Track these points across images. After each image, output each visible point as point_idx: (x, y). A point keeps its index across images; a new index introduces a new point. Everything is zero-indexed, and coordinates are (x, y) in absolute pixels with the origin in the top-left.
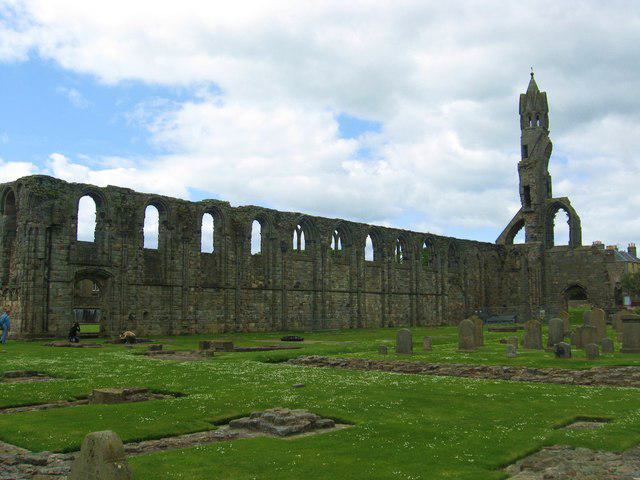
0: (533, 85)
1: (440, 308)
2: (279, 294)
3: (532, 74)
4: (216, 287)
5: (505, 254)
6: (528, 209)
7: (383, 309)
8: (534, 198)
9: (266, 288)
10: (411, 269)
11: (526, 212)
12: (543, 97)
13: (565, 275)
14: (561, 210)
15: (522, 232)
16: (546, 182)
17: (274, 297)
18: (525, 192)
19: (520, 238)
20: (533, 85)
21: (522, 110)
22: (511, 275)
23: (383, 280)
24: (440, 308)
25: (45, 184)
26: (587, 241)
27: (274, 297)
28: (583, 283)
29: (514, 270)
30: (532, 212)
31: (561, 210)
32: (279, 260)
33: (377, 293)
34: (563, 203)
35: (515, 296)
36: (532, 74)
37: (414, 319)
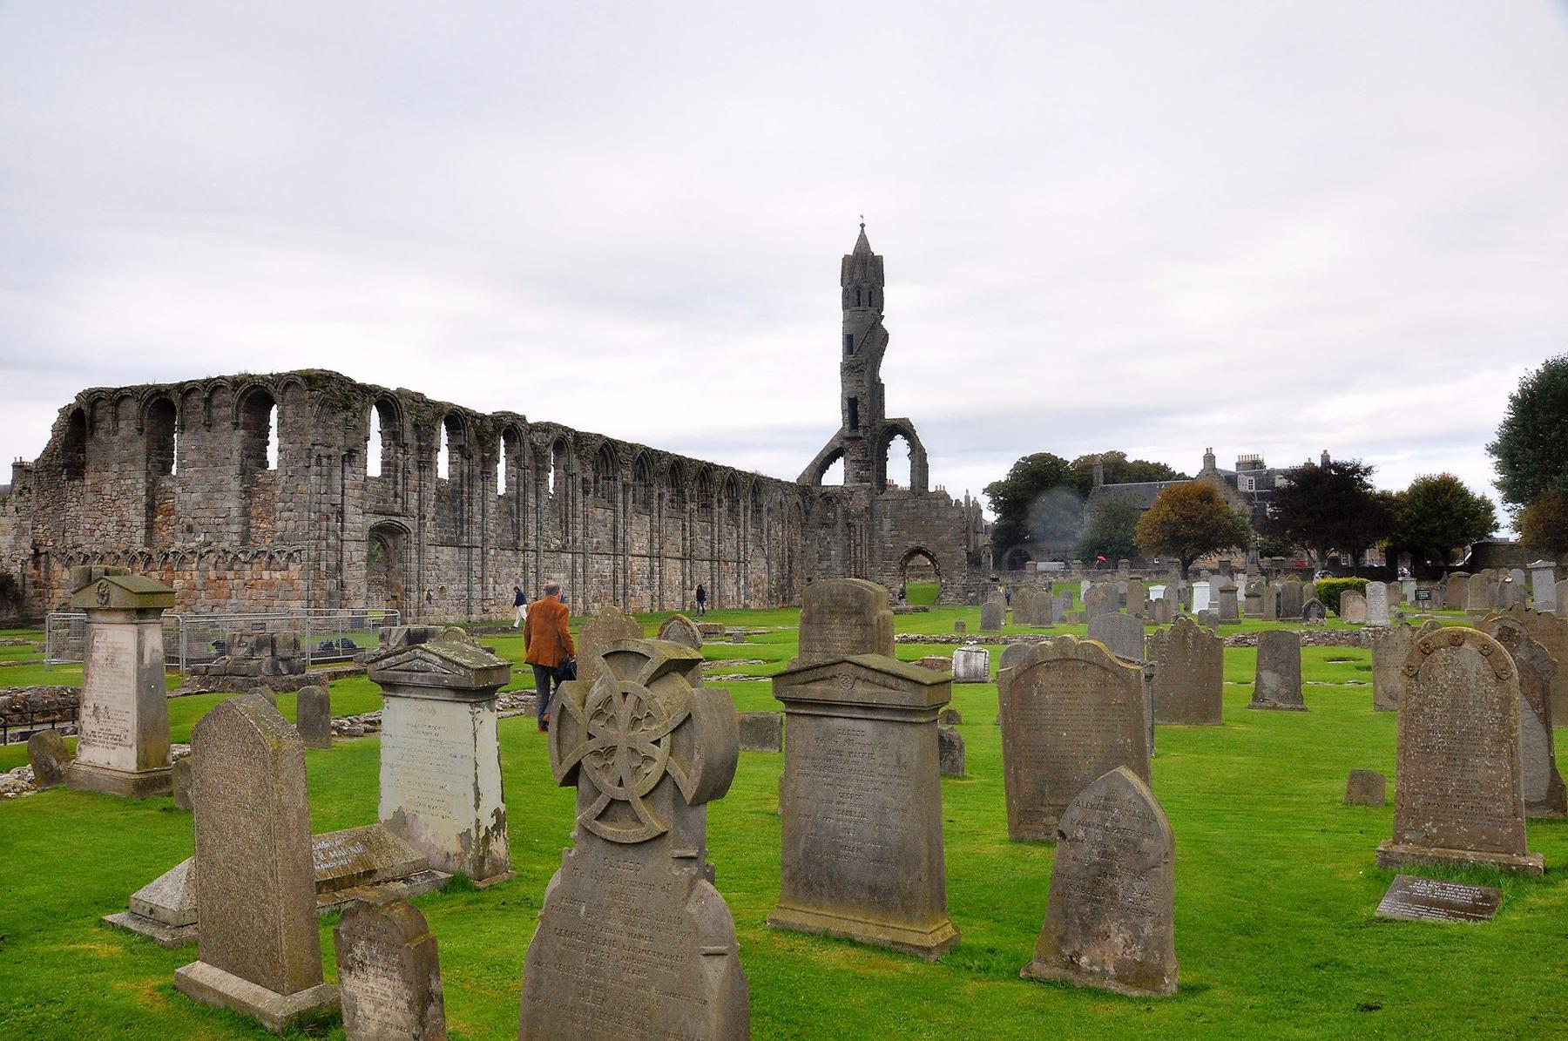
0: (863, 242)
1: (742, 583)
2: (580, 561)
3: (862, 226)
4: (515, 548)
6: (853, 434)
7: (684, 582)
8: (863, 422)
9: (563, 550)
11: (848, 439)
14: (899, 437)
16: (877, 390)
17: (574, 563)
18: (852, 406)
19: (835, 476)
20: (863, 242)
21: (847, 280)
24: (742, 583)
25: (334, 386)
26: (934, 482)
27: (574, 563)
28: (930, 548)
30: (861, 438)
31: (899, 437)
32: (580, 506)
33: (678, 558)
34: (903, 428)
35: (825, 564)
36: (862, 226)
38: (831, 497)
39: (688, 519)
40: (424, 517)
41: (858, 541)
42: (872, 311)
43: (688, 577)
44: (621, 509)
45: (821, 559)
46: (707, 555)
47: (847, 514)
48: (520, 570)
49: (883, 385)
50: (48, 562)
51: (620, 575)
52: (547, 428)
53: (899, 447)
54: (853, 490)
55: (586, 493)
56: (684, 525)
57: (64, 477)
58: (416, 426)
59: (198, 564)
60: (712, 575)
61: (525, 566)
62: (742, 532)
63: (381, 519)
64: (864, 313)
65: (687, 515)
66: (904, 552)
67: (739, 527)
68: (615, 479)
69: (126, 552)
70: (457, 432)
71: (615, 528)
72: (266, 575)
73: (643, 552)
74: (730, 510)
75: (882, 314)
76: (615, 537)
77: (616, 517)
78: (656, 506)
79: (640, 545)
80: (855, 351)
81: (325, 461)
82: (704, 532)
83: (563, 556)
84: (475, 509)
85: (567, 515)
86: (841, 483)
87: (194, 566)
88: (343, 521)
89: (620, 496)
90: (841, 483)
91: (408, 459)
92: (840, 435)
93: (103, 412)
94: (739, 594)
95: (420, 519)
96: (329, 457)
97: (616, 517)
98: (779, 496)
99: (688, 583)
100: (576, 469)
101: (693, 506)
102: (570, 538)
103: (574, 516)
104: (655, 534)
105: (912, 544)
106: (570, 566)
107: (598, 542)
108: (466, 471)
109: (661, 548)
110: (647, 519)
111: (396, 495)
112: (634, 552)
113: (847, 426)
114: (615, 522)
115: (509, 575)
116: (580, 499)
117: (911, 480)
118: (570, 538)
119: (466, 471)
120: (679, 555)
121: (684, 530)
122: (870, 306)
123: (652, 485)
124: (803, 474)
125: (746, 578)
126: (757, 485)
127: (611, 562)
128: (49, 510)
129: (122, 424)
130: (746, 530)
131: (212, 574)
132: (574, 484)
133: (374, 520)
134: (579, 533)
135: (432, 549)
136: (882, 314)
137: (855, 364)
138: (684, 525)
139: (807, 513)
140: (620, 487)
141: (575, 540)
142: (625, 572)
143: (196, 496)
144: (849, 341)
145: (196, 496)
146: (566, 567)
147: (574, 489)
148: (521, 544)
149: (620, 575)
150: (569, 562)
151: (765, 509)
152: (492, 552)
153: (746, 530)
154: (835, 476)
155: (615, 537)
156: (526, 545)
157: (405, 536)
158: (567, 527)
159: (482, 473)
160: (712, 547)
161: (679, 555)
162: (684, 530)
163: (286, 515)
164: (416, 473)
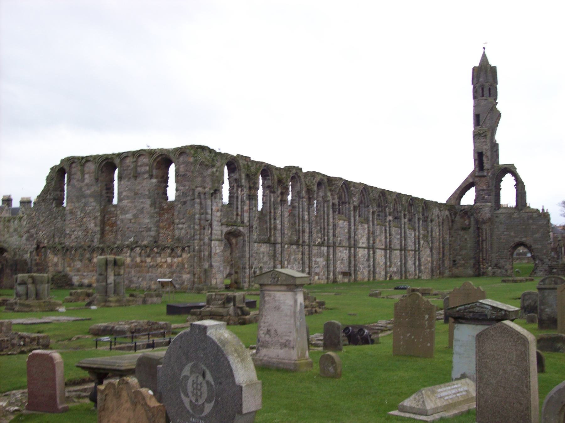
1: (417, 263)
2: (331, 250)
3: (484, 48)
4: (297, 243)
5: (455, 214)
6: (481, 174)
7: (386, 263)
8: (487, 166)
10: (401, 228)
12: (493, 70)
13: (512, 234)
15: (472, 191)
16: (495, 147)
17: (328, 252)
18: (479, 157)
19: (469, 199)
21: (475, 82)
22: (461, 233)
23: (386, 238)
29: (465, 229)
30: (484, 176)
32: (331, 220)
34: (510, 169)
36: (484, 48)
37: (403, 272)
38: (468, 211)
39: (388, 226)
40: (252, 227)
41: (484, 238)
42: (490, 99)
43: (388, 260)
44: (352, 221)
45: (461, 249)
46: (398, 247)
47: (477, 222)
48: (300, 256)
49: (498, 144)
50: (46, 252)
51: (352, 259)
52: (314, 174)
53: (508, 182)
54: (481, 207)
55: (334, 212)
56: (386, 230)
57: (54, 205)
58: (247, 176)
59: (130, 253)
60: (401, 259)
61: (303, 254)
62: (417, 234)
63: (230, 228)
64: (486, 101)
65: (387, 224)
66: (512, 244)
67: (415, 230)
68: (349, 203)
69: (89, 247)
70: (268, 178)
71: (349, 232)
72: (169, 260)
73: (364, 245)
74: (410, 220)
75: (497, 101)
76: (350, 237)
77: (350, 225)
78: (371, 219)
79: (363, 241)
80: (481, 123)
81: (202, 196)
82: (397, 234)
83: (322, 248)
84: (278, 222)
85: (324, 225)
86: (472, 203)
87: (128, 254)
88: (211, 230)
89: (352, 213)
90: (472, 203)
91: (243, 194)
92: (472, 175)
93: (75, 169)
94: (415, 270)
95: (250, 228)
96: (205, 194)
97: (350, 225)
98: (436, 211)
99: (388, 263)
100: (330, 198)
101: (390, 218)
102: (326, 238)
103: (328, 225)
104: (371, 235)
105: (517, 240)
106: (326, 254)
107: (340, 240)
108: (272, 200)
109: (374, 243)
110: (366, 226)
111: (237, 215)
112: (360, 245)
113: (477, 169)
114: (350, 229)
115: (295, 260)
116: (331, 216)
117: (517, 201)
118: (326, 238)
119: (272, 200)
120: (383, 247)
121: (386, 232)
122: (490, 96)
123: (368, 206)
124: (450, 198)
125: (419, 260)
126: (427, 205)
127: (347, 252)
128: (46, 223)
129: (87, 176)
130: (419, 232)
131: (138, 260)
132: (328, 207)
133: (225, 229)
134: (331, 234)
135: (256, 244)
136: (497, 101)
137: (481, 132)
138: (386, 230)
139: (453, 221)
140: (352, 208)
141: (328, 239)
142: (355, 257)
143: (129, 216)
144: (477, 118)
145: (129, 216)
146: (324, 255)
147: (328, 210)
148: (301, 242)
149: (352, 259)
150: (325, 251)
151: (429, 220)
152: (286, 246)
153: (419, 232)
154: (469, 199)
155: (350, 237)
156: (304, 242)
157: (242, 237)
158: (324, 231)
159: (281, 201)
160: (401, 242)
161: (383, 247)
162: (386, 232)
163: (180, 226)
164: (247, 202)
